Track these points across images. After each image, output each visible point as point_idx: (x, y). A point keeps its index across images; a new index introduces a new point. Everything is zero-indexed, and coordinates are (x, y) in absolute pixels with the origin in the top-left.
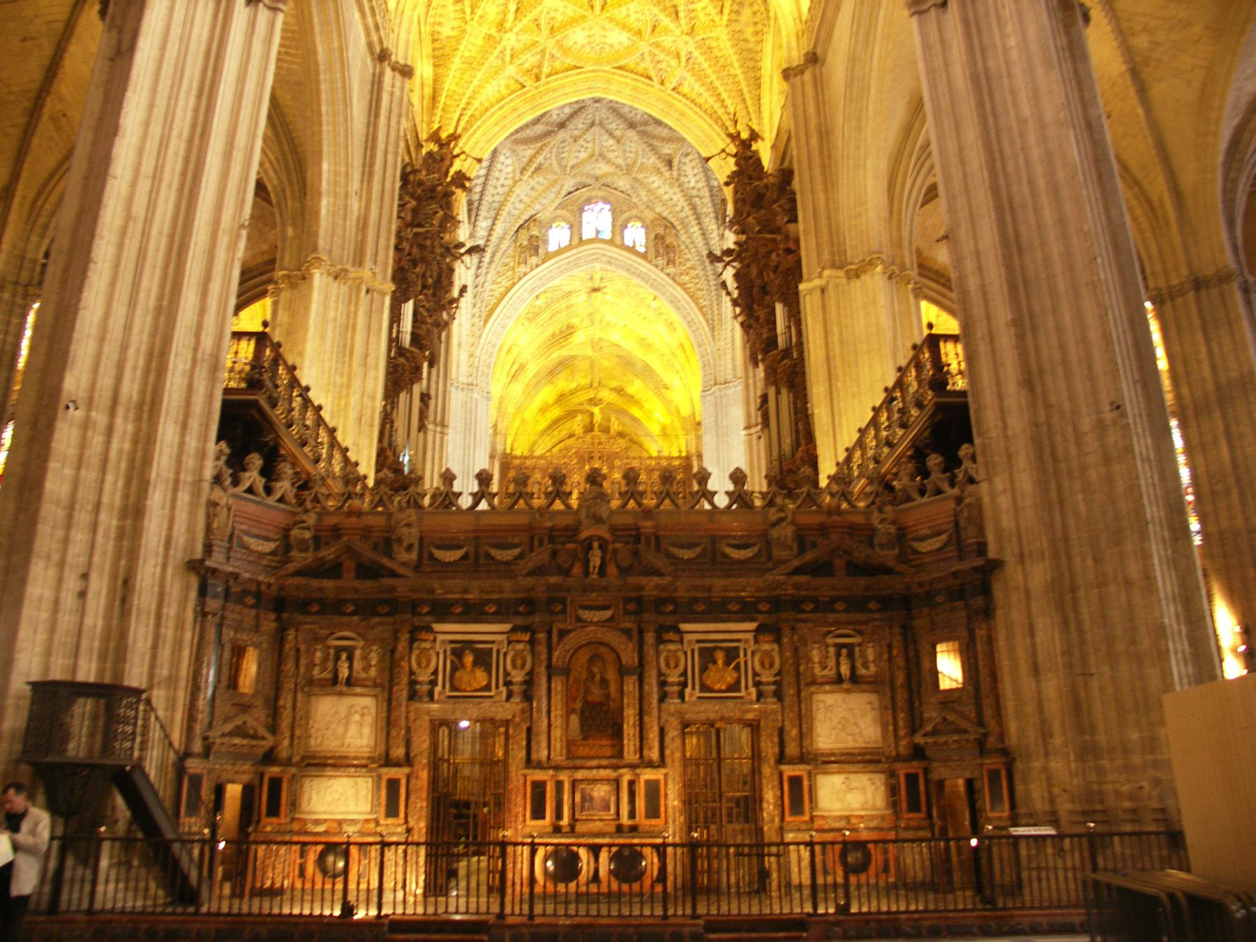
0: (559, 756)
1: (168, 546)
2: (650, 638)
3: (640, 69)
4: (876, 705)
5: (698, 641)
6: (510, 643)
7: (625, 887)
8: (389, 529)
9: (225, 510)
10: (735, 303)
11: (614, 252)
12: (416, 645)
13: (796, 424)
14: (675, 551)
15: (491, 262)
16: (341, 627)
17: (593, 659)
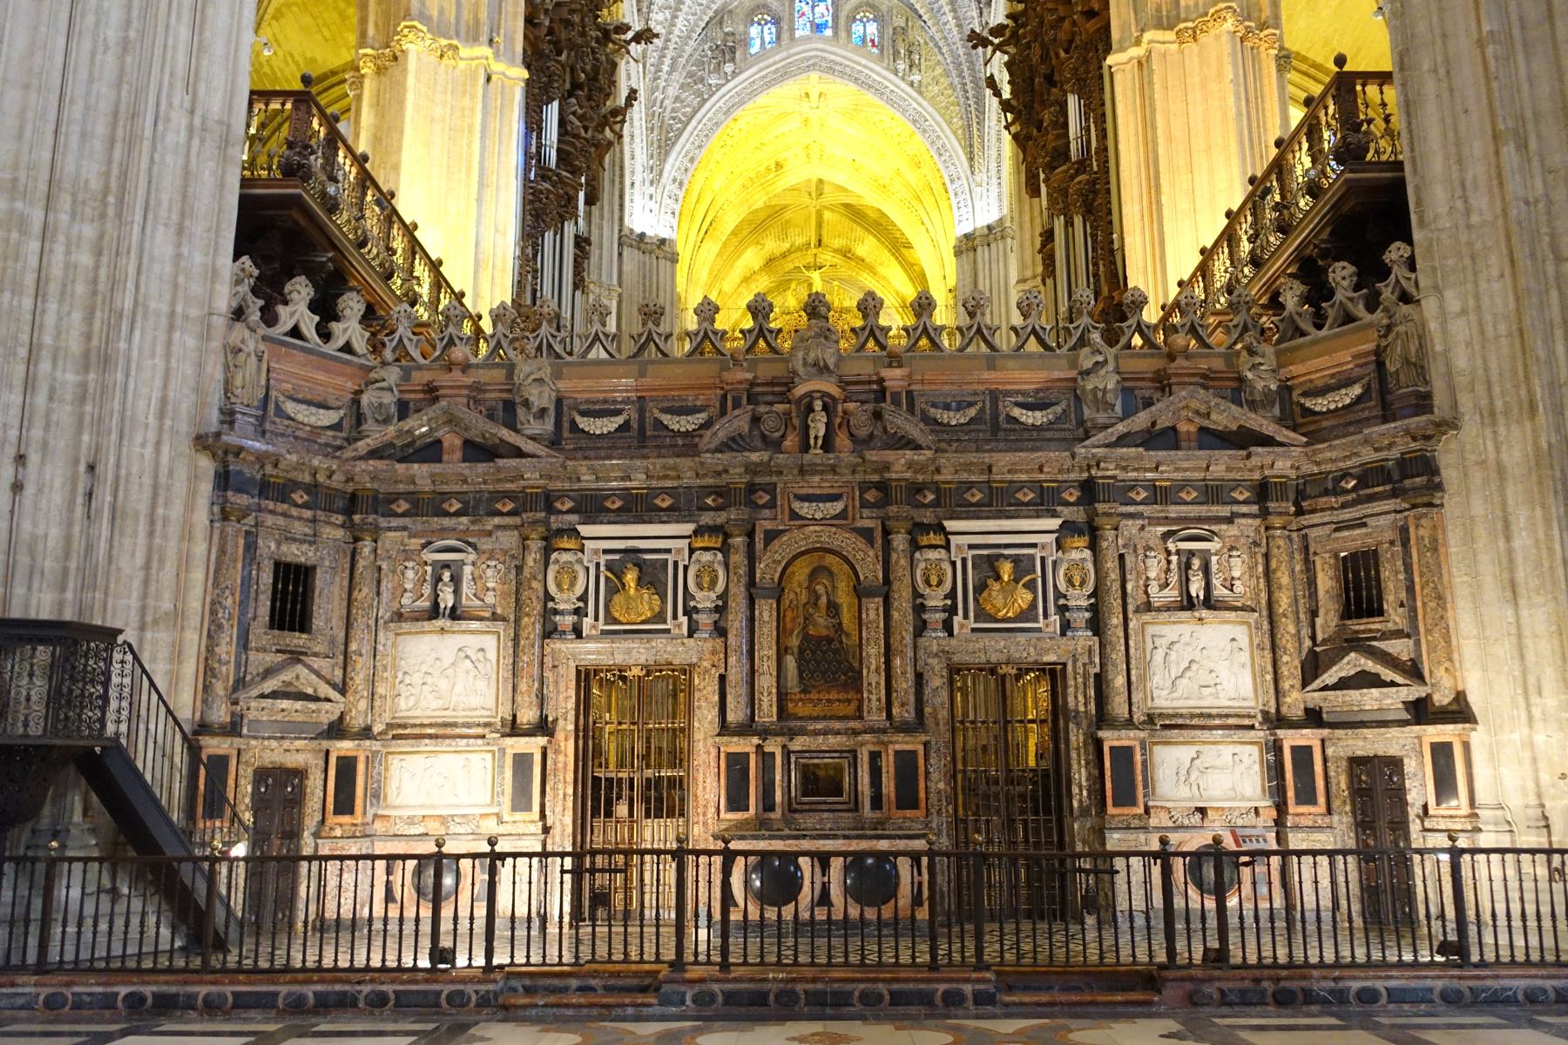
1: (161, 416)
2: (900, 541)
4: (1244, 641)
5: (971, 547)
6: (692, 551)
7: (871, 914)
8: (511, 385)
9: (253, 358)
10: (1006, 106)
11: (840, 53)
12: (554, 556)
13: (1096, 265)
14: (937, 413)
15: (669, 73)
16: (443, 532)
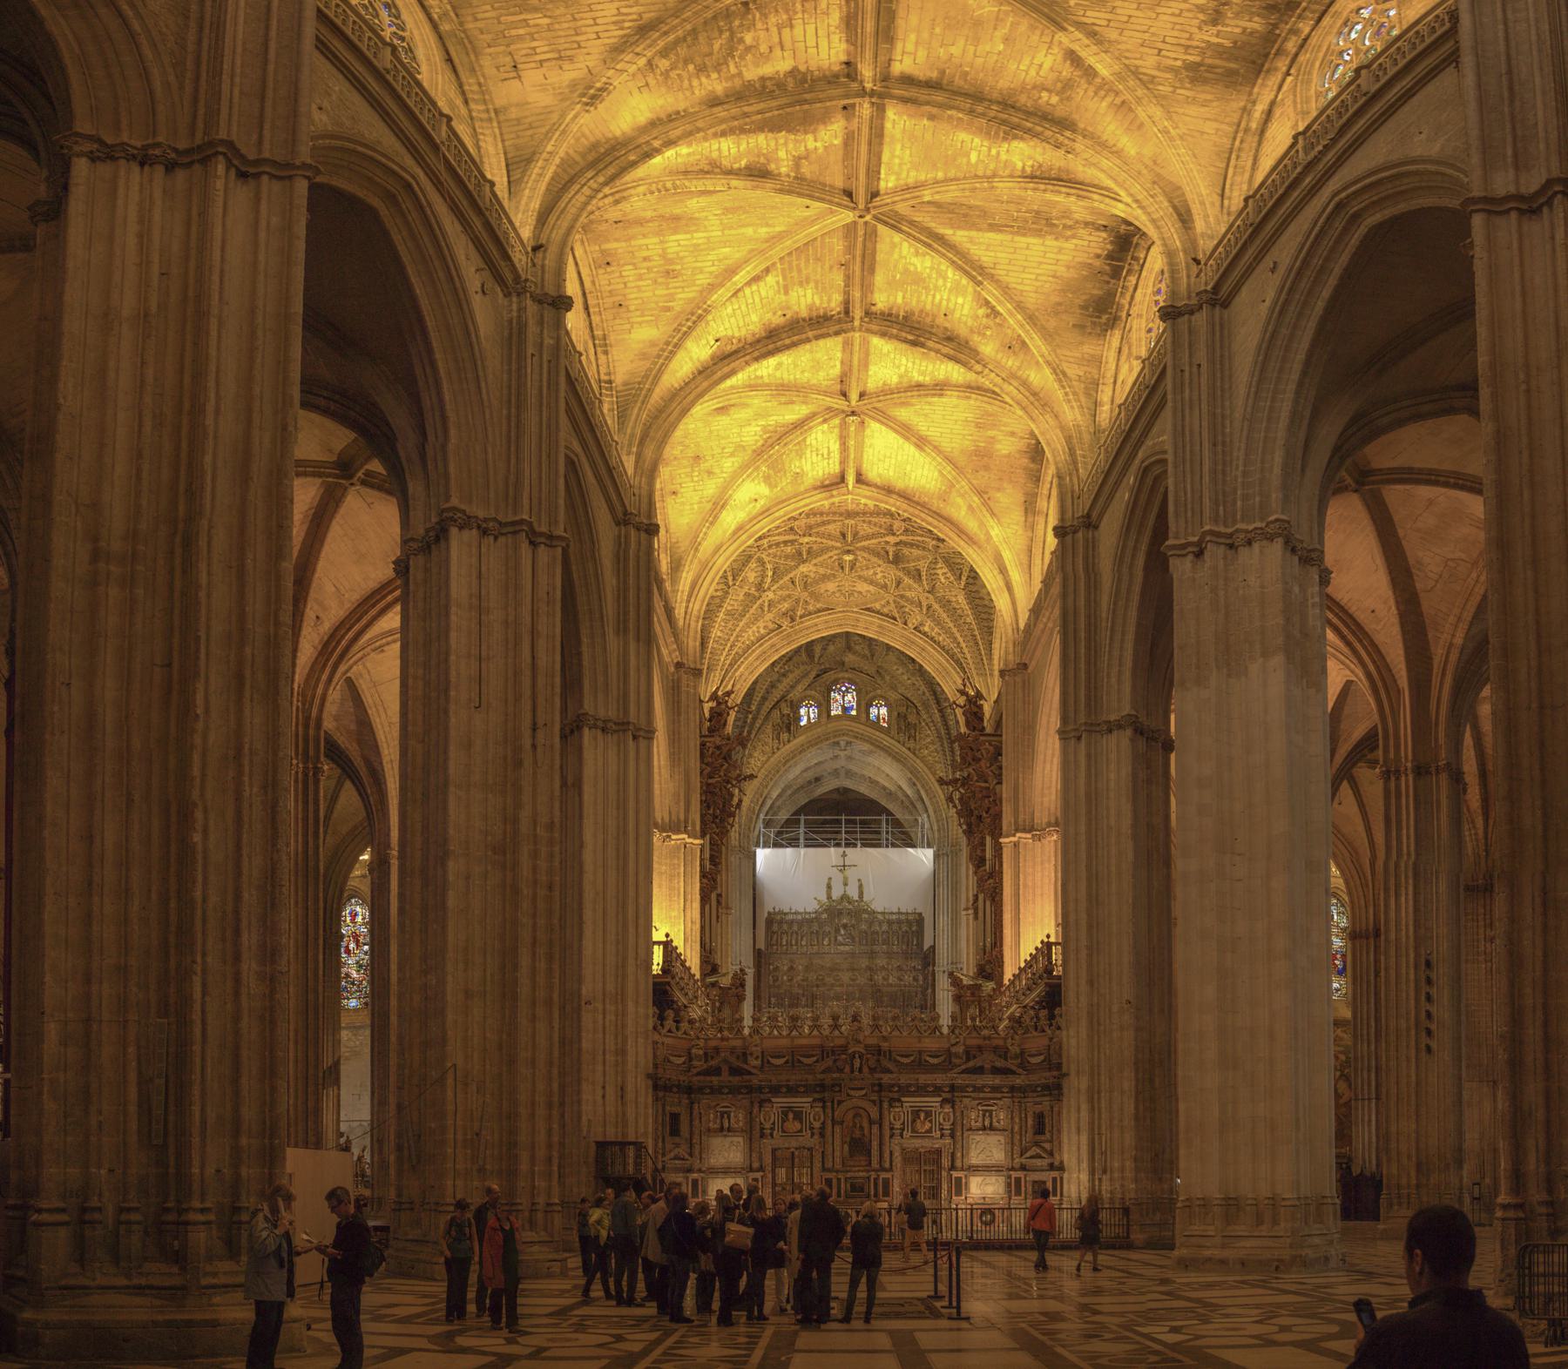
0: (839, 1166)
2: (886, 1105)
3: (885, 610)
17: (856, 1115)
